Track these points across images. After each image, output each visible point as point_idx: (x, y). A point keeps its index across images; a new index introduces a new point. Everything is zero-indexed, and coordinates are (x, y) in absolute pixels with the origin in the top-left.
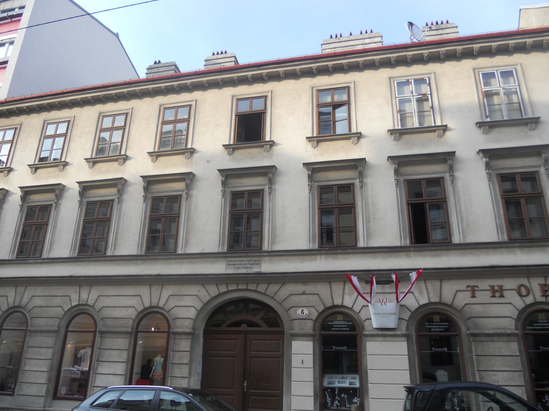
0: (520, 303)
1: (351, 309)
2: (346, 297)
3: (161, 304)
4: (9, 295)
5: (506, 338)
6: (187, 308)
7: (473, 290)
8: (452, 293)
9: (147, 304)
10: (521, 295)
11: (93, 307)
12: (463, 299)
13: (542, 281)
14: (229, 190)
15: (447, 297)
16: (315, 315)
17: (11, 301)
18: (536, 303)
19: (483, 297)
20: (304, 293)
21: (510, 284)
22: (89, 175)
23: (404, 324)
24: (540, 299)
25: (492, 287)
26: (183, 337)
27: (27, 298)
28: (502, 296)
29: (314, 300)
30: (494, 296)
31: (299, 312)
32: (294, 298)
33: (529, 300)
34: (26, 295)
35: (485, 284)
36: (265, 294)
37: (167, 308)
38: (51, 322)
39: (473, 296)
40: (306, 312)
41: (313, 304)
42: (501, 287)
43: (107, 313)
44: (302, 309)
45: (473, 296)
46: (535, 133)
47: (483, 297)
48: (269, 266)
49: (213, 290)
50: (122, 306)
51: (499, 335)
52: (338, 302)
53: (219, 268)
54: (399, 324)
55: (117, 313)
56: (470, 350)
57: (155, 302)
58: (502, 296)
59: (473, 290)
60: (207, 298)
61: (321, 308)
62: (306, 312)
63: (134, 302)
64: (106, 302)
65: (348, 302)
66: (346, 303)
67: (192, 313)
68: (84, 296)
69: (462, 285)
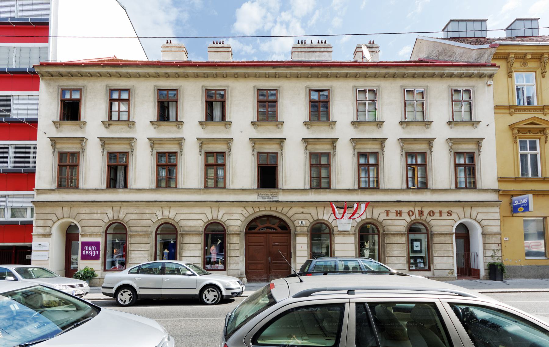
0: (408, 219)
1: (327, 221)
2: (325, 215)
3: (219, 218)
4: (108, 212)
6: (235, 221)
7: (387, 213)
8: (378, 214)
9: (210, 218)
10: (410, 216)
11: (173, 220)
12: (383, 217)
13: (420, 209)
14: (356, 151)
15: (375, 216)
16: (308, 224)
17: (111, 216)
18: (416, 219)
19: (392, 216)
20: (302, 213)
21: (405, 210)
22: (154, 133)
23: (354, 229)
24: (418, 217)
25: (397, 211)
26: (235, 236)
27: (123, 214)
28: (401, 216)
29: (308, 216)
30: (397, 216)
31: (300, 222)
32: (297, 215)
33: (413, 218)
34: (121, 212)
35: (393, 210)
36: (281, 213)
37: (223, 220)
38: (236, 228)
39: (387, 216)
40: (304, 222)
41: (307, 218)
42: (400, 211)
43: (183, 223)
44: (302, 221)
45: (387, 216)
47: (392, 216)
48: (282, 197)
49: (251, 211)
50: (194, 220)
51: (397, 234)
52: (320, 217)
53: (254, 197)
54: (351, 229)
55: (191, 223)
56: (384, 241)
57: (215, 216)
58: (401, 216)
59: (387, 213)
60: (247, 215)
61: (312, 221)
62: (304, 222)
63: (202, 217)
64: (182, 217)
65: (326, 218)
66: (319, 218)
67: (239, 223)
68: (166, 213)
69: (383, 210)
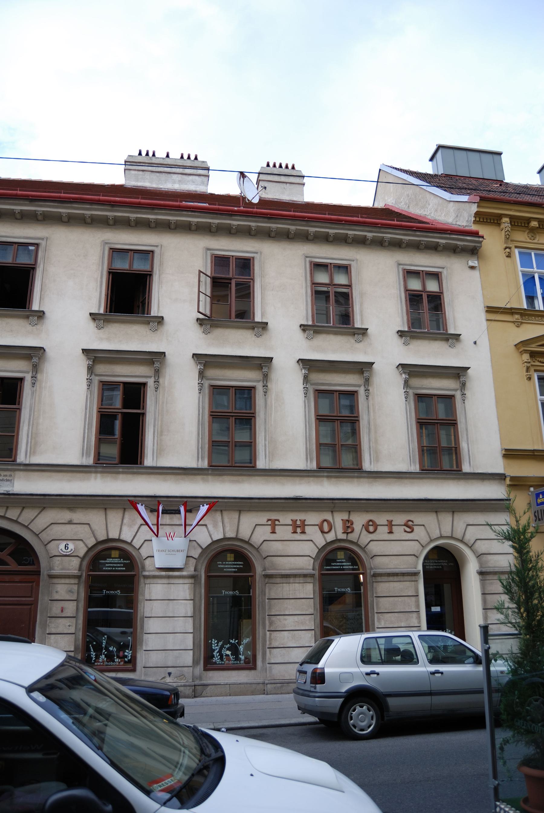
0: (320, 541)
1: (130, 544)
2: (125, 528)
5: (302, 580)
7: (273, 524)
8: (250, 527)
10: (323, 532)
12: (261, 535)
13: (345, 516)
15: (245, 534)
16: (82, 551)
20: (70, 523)
21: (313, 518)
23: (192, 562)
25: (294, 522)
28: (303, 532)
29: (82, 532)
30: (295, 532)
31: (62, 546)
32: (55, 528)
33: (330, 537)
35: (286, 518)
36: (16, 522)
40: (71, 546)
41: (81, 536)
45: (273, 532)
46: (360, 346)
48: (23, 485)
51: (295, 576)
52: (113, 534)
54: (186, 564)
56: (263, 593)
58: (303, 532)
59: (273, 524)
61: (91, 542)
65: (127, 536)
66: (123, 537)
69: (262, 518)
